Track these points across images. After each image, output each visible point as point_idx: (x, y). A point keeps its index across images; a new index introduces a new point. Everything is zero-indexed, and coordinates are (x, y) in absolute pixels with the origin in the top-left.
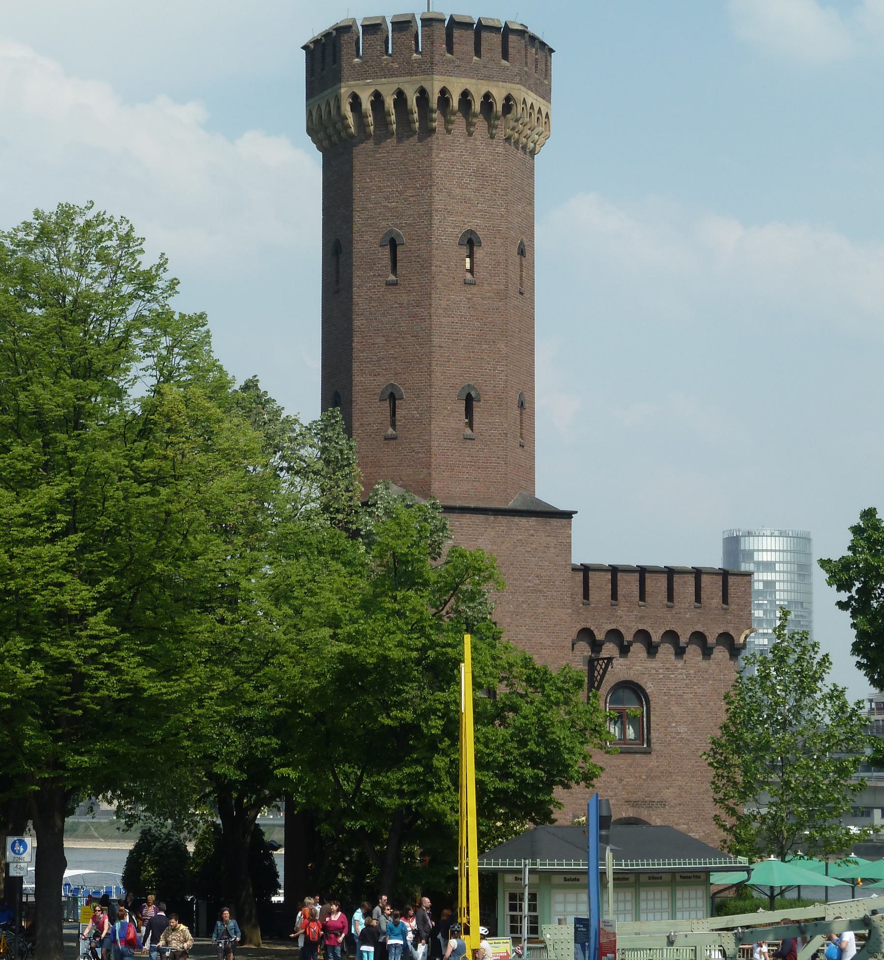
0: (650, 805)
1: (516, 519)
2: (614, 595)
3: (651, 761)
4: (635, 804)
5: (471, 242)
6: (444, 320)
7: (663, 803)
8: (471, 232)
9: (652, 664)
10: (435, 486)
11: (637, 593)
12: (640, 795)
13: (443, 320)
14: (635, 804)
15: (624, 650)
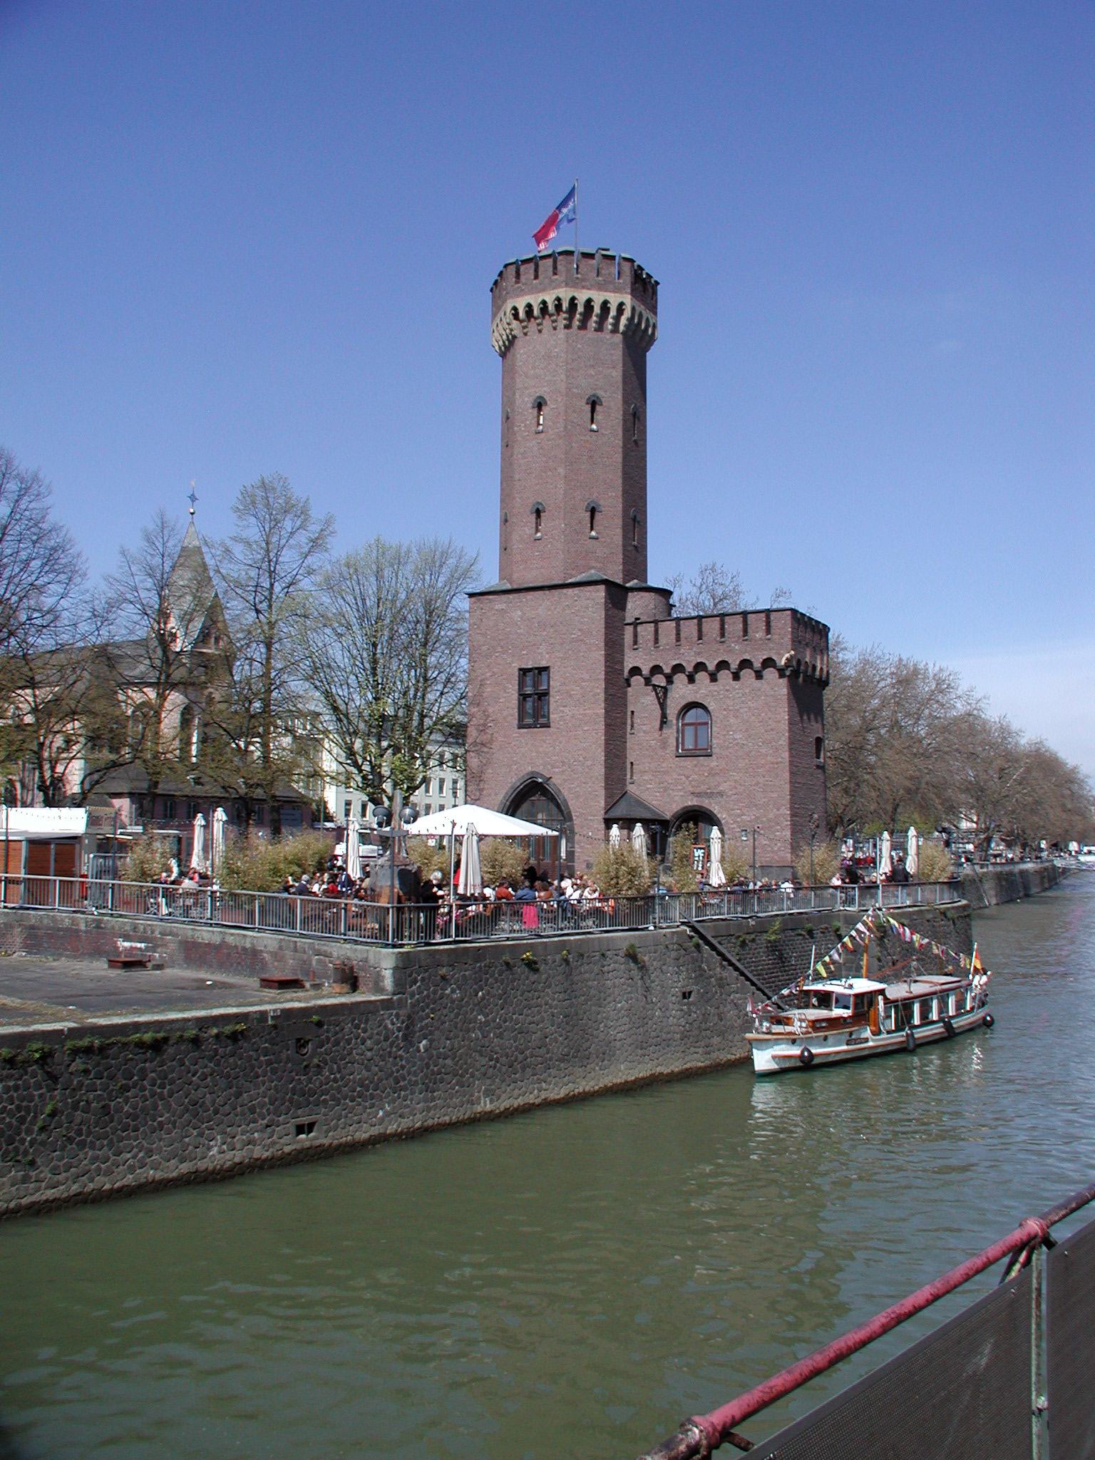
0: (710, 795)
1: (565, 591)
2: (678, 639)
3: (713, 762)
4: (698, 795)
5: (540, 405)
6: (522, 462)
7: (721, 794)
8: (541, 397)
9: (714, 687)
10: (515, 576)
11: (695, 634)
12: (703, 788)
13: (522, 462)
14: (698, 795)
15: (691, 679)
